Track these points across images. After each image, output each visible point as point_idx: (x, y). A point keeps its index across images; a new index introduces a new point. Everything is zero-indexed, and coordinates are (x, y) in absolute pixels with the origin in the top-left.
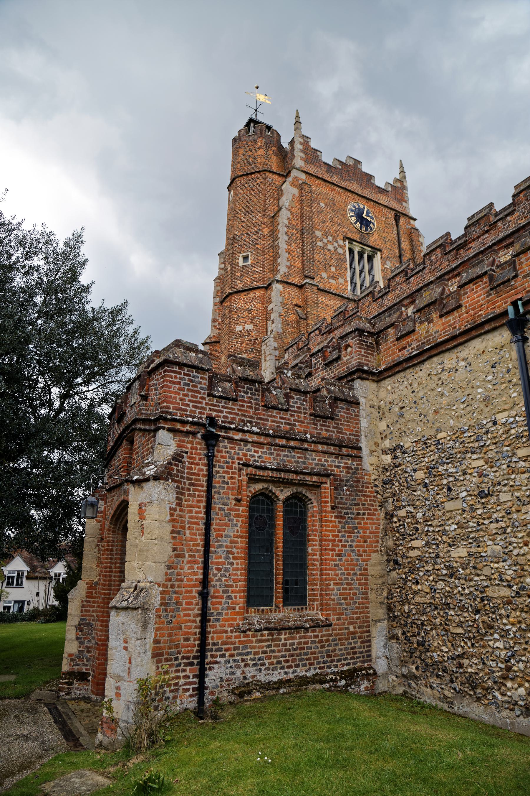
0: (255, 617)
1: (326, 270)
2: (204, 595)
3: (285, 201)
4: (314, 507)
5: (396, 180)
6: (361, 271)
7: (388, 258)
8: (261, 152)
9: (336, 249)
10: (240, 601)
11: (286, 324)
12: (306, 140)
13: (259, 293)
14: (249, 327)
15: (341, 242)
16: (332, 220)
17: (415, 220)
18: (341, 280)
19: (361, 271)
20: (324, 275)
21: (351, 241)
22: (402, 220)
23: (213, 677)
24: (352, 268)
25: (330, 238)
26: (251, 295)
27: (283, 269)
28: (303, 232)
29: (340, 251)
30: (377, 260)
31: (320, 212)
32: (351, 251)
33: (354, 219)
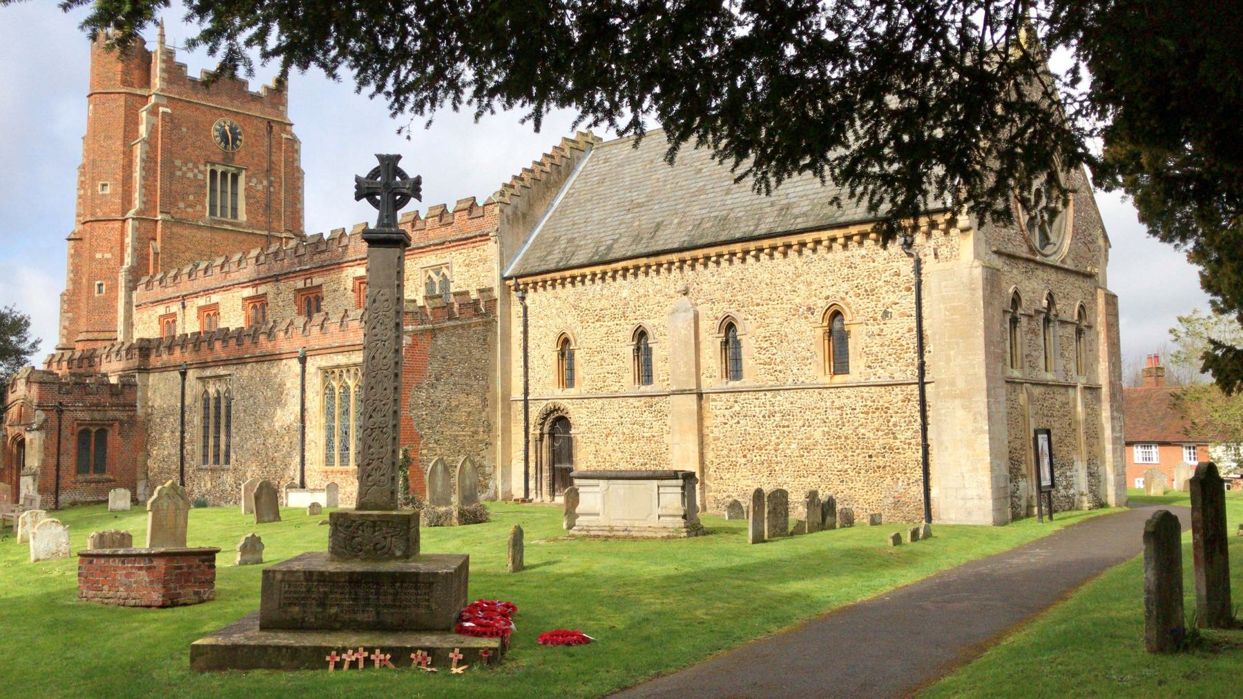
0: (80, 477)
1: (183, 199)
2: (58, 470)
4: (110, 433)
6: (223, 192)
7: (254, 175)
9: (195, 176)
10: (73, 472)
13: (118, 225)
14: (108, 256)
15: (202, 167)
16: (193, 145)
17: (291, 125)
18: (199, 208)
19: (223, 192)
20: (182, 205)
21: (213, 164)
22: (276, 128)
23: (61, 498)
24: (213, 190)
25: (190, 165)
26: (110, 225)
29: (200, 177)
31: (181, 139)
32: (213, 173)
33: (219, 139)
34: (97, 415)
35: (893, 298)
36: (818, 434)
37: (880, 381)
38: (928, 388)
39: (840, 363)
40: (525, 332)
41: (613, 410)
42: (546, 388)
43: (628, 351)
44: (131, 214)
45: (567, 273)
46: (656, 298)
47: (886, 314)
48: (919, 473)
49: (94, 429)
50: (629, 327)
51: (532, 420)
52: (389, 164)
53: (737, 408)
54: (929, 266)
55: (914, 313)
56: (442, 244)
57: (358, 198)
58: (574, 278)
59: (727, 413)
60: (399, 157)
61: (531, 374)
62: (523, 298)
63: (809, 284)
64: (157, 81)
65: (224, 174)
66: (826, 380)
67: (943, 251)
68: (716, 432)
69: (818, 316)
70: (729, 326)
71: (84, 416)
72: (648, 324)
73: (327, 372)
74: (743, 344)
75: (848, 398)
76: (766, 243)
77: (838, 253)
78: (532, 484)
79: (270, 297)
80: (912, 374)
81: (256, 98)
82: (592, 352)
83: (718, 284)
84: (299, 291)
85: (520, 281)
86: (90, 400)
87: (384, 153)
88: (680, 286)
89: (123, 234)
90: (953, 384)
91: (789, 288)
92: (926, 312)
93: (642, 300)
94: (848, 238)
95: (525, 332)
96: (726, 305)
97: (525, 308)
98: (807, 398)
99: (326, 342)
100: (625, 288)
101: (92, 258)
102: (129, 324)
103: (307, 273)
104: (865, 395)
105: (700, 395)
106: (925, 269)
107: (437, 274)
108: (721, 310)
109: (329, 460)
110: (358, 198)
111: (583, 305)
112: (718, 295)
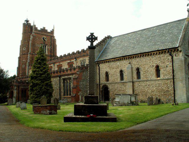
3: (31, 39)
5: (53, 30)
8: (27, 28)
11: (30, 61)
12: (35, 26)
13: (26, 55)
15: (40, 45)
21: (42, 44)
22: (52, 38)
27: (30, 51)
28: (33, 45)
30: (47, 46)
34: (24, 87)
35: (168, 63)
36: (155, 88)
37: (166, 79)
38: (175, 80)
39: (158, 75)
40: (99, 72)
41: (116, 86)
42: (103, 81)
43: (119, 75)
44: (29, 53)
45: (107, 60)
46: (125, 65)
47: (167, 66)
48: (173, 95)
49: (24, 90)
50: (119, 70)
51: (101, 87)
52: (92, 34)
53: (140, 84)
54: (174, 57)
55: (172, 66)
56: (84, 56)
57: (87, 40)
58: (108, 61)
59: (138, 85)
60: (94, 33)
61: (100, 79)
62: (99, 65)
63: (153, 61)
64: (33, 31)
65: (44, 46)
66: (156, 78)
67: (177, 55)
68: (136, 89)
69: (154, 67)
70: (138, 69)
71: (22, 87)
72: (123, 69)
73: (64, 80)
74: (141, 72)
75: (160, 82)
76: (145, 54)
77: (158, 56)
78: (101, 99)
79: (53, 66)
80: (172, 77)
81: (49, 33)
82: (112, 75)
83: (136, 63)
84: (58, 65)
85: (98, 62)
86: (24, 85)
87: (91, 33)
88: (129, 62)
89: (27, 57)
90: (179, 79)
91: (149, 62)
92: (174, 66)
93: (121, 65)
94: (159, 53)
95: (99, 72)
96: (137, 65)
97: (99, 67)
98: (152, 82)
99: (64, 74)
100: (118, 63)
101: (22, 61)
102: (28, 72)
103: (59, 62)
104: (163, 81)
105: (133, 82)
106: (174, 58)
107: (83, 61)
108: (137, 66)
109: (64, 95)
110: (87, 40)
111: (110, 66)
112: (136, 64)
